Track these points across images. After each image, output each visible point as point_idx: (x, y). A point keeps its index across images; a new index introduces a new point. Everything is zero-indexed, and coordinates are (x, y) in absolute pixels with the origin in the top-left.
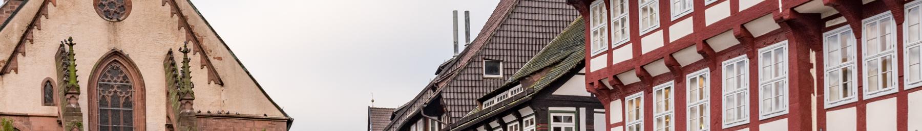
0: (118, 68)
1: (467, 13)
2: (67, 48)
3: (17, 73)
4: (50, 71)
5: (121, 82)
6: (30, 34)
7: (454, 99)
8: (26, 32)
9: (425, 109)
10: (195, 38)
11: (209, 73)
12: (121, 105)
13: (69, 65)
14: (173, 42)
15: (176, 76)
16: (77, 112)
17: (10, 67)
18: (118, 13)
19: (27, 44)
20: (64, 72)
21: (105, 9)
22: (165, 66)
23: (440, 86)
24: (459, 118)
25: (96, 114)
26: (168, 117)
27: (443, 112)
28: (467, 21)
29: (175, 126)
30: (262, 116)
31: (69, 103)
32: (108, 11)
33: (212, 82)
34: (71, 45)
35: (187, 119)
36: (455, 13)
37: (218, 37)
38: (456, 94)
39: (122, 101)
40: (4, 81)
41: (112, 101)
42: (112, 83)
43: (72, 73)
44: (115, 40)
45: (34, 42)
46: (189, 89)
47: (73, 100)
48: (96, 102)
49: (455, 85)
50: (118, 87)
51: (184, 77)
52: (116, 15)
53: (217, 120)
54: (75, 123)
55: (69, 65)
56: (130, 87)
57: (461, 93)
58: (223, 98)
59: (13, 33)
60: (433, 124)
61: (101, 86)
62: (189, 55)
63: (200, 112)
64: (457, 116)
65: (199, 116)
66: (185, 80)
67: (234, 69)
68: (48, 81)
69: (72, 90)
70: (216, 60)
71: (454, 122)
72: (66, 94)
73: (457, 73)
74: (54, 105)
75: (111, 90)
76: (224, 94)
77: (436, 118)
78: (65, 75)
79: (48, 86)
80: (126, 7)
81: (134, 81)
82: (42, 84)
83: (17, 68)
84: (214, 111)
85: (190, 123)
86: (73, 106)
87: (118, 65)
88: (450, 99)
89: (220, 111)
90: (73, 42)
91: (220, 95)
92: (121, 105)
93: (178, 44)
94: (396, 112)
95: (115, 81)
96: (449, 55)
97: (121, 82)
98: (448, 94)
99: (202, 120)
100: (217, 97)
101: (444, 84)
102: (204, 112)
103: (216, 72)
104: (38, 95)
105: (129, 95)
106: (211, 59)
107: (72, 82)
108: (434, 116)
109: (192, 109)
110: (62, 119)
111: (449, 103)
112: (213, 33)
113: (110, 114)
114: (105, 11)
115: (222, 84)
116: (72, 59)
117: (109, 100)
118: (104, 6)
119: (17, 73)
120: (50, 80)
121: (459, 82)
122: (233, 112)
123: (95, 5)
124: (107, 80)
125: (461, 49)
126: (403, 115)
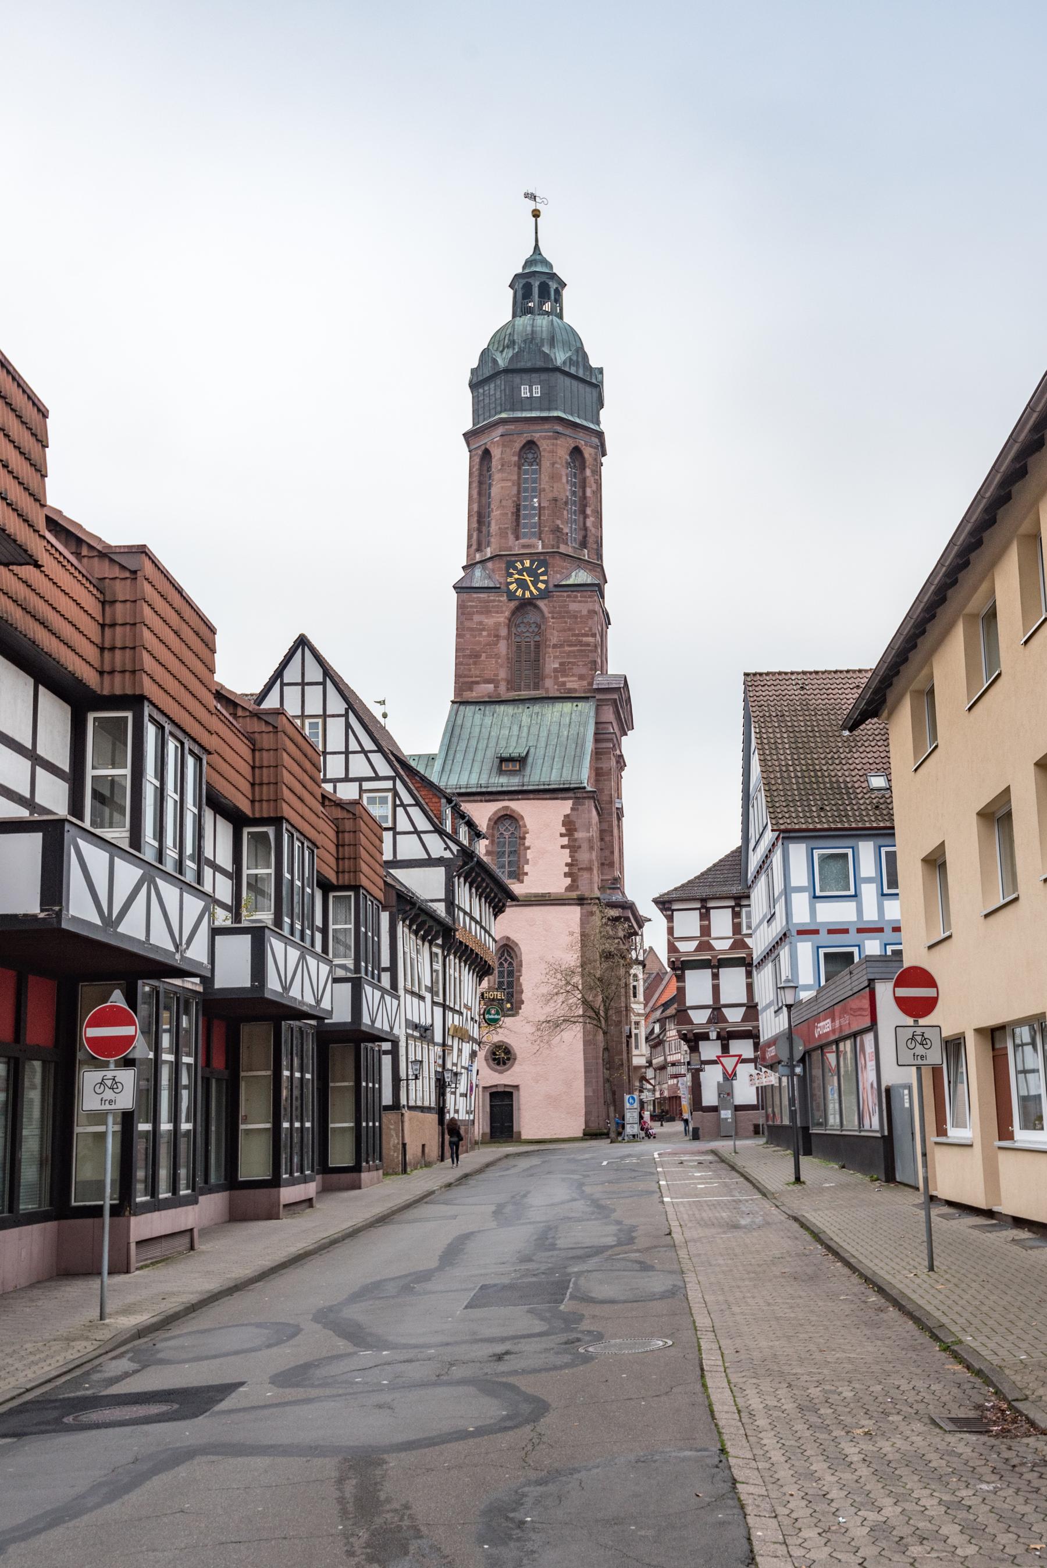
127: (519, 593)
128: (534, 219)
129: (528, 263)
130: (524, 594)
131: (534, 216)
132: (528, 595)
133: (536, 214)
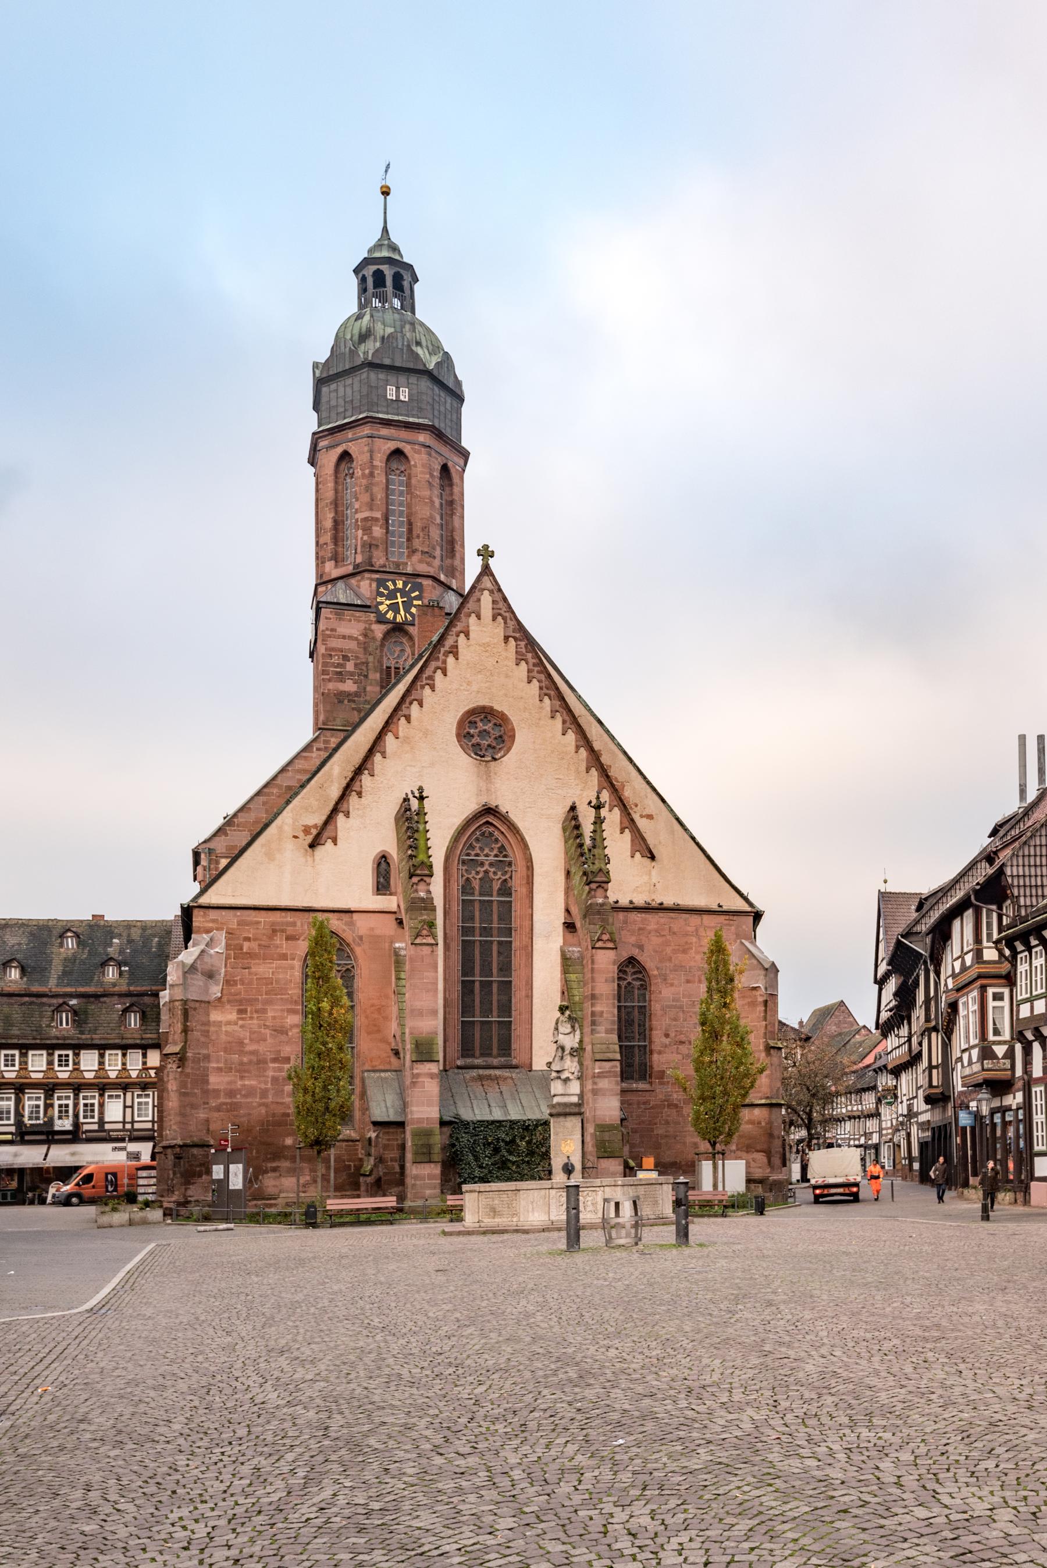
0: (491, 834)
1: (1041, 738)
2: (414, 804)
3: (336, 844)
4: (386, 840)
5: (496, 856)
6: (358, 783)
7: (1024, 876)
8: (352, 779)
9: (976, 892)
10: (613, 785)
11: (632, 841)
12: (495, 893)
13: (417, 831)
14: (578, 792)
15: (581, 845)
16: (427, 905)
17: (326, 834)
18: (494, 748)
19: (353, 799)
20: (410, 842)
21: (474, 741)
22: (564, 830)
23: (1002, 855)
24: (1032, 906)
25: (456, 908)
26: (568, 911)
27: (1005, 897)
28: (1041, 751)
29: (578, 925)
30: (715, 907)
31: (416, 891)
32: (478, 744)
33: (638, 855)
34: (421, 798)
35: (599, 913)
36: (1022, 738)
37: (649, 783)
38: (1027, 868)
39: (496, 886)
41: (481, 887)
42: (482, 858)
43: (422, 842)
44: (488, 790)
46: (603, 866)
47: (422, 886)
48: (456, 888)
49: (1026, 853)
50: (491, 865)
51: (594, 847)
52: (490, 750)
53: (643, 915)
54: (424, 921)
55: (417, 831)
56: (510, 864)
57: (1035, 866)
58: (654, 881)
59: (332, 781)
60: (989, 916)
61: (464, 862)
62: (604, 812)
63: (617, 902)
64: (1028, 903)
65: (617, 908)
66: (596, 851)
67: (672, 832)
68: (384, 857)
69: (419, 871)
70: (644, 819)
71: (1023, 913)
72: (411, 876)
73: (1029, 834)
74: (391, 894)
75: (479, 869)
76: (656, 872)
77: (994, 907)
78: (410, 847)
79: (383, 862)
80: (506, 738)
81: (515, 854)
84: (639, 900)
85: (603, 920)
86: (422, 894)
87: (491, 829)
88: (1018, 876)
89: (649, 900)
90: (425, 794)
91: (650, 874)
92: (495, 893)
93: (585, 794)
94: (926, 899)
95: (487, 855)
96: (1012, 806)
97: (496, 856)
98: (1015, 868)
99: (621, 915)
100: (646, 878)
101: (1008, 852)
102: (624, 902)
103: (644, 839)
105: (507, 877)
106: (636, 817)
107: (422, 857)
108: (991, 904)
109: (606, 897)
110: (403, 916)
111: (1016, 883)
112: (639, 777)
113: (477, 906)
114: (473, 745)
115: (653, 858)
116: (422, 821)
117: (476, 884)
118: (473, 736)
119: (336, 844)
121: (1032, 849)
122: (669, 901)
124: (473, 853)
125: (1032, 795)
126: (937, 902)
127: (390, 615)
128: (383, 197)
129: (378, 246)
130: (395, 617)
131: (383, 193)
132: (399, 619)
133: (386, 192)
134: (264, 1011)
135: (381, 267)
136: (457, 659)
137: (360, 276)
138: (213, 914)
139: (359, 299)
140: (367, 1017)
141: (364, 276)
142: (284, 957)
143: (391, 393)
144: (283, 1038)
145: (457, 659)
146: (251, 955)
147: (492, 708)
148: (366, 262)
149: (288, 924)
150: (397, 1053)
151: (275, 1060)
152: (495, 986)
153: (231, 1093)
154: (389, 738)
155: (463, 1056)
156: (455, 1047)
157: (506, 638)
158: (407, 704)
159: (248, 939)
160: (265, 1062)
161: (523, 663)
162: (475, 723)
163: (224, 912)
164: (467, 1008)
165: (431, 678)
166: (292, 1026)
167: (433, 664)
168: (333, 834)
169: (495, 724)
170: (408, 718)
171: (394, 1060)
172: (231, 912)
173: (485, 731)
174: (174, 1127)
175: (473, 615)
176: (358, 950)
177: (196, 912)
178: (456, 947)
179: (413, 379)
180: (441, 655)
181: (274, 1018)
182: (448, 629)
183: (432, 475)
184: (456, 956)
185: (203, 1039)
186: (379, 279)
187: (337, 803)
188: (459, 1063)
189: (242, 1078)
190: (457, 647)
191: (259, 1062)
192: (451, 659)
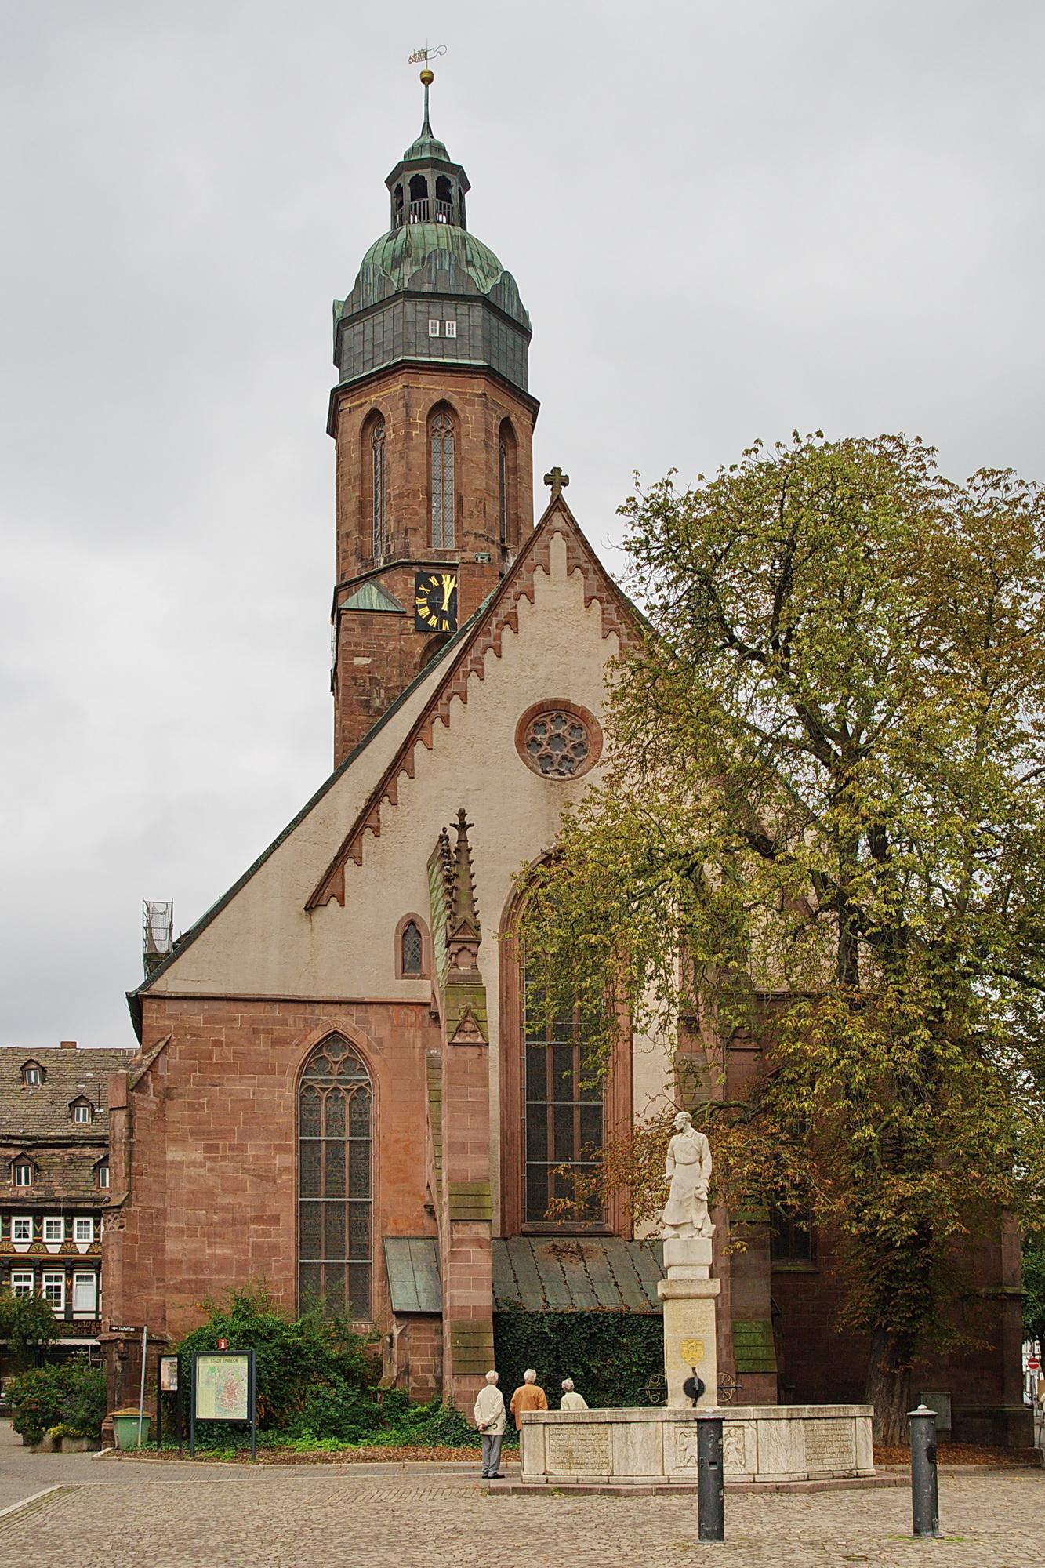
3: (342, 905)
6: (374, 816)
18: (571, 761)
21: (541, 751)
40: (316, 925)
45: (382, 832)
68: (412, 923)
74: (422, 977)
79: (410, 929)
80: (588, 745)
82: (397, 932)
83: (343, 893)
104: (389, 953)
114: (540, 758)
118: (540, 745)
119: (342, 905)
120: (417, 920)
123: (520, 743)
134: (242, 1148)
135: (420, 172)
136: (516, 633)
137: (395, 186)
138: (171, 1007)
139: (394, 217)
140: (389, 1158)
141: (399, 185)
142: (270, 1069)
143: (434, 329)
144: (270, 1187)
145: (516, 633)
146: (224, 1067)
147: (567, 703)
148: (400, 169)
149: (275, 1021)
150: (431, 1212)
151: (258, 1219)
152: (576, 1114)
153: (197, 1267)
154: (419, 749)
155: (530, 1218)
156: (519, 1203)
157: (588, 601)
158: (445, 701)
159: (218, 1043)
160: (244, 1222)
161: (613, 635)
162: (544, 725)
163: (185, 1005)
164: (535, 1147)
165: (479, 661)
166: (282, 1171)
167: (482, 641)
168: (338, 890)
169: (573, 727)
170: (446, 721)
171: (427, 1221)
172: (194, 1007)
173: (558, 736)
174: (115, 1313)
175: (539, 568)
176: (375, 1059)
177: (146, 1004)
178: (518, 1055)
179: (463, 308)
180: (492, 628)
181: (256, 1158)
182: (502, 590)
183: (487, 432)
184: (519, 1071)
185: (155, 1187)
186: (419, 187)
187: (344, 846)
188: (526, 1227)
189: (211, 1245)
190: (516, 614)
191: (234, 1222)
192: (507, 633)
